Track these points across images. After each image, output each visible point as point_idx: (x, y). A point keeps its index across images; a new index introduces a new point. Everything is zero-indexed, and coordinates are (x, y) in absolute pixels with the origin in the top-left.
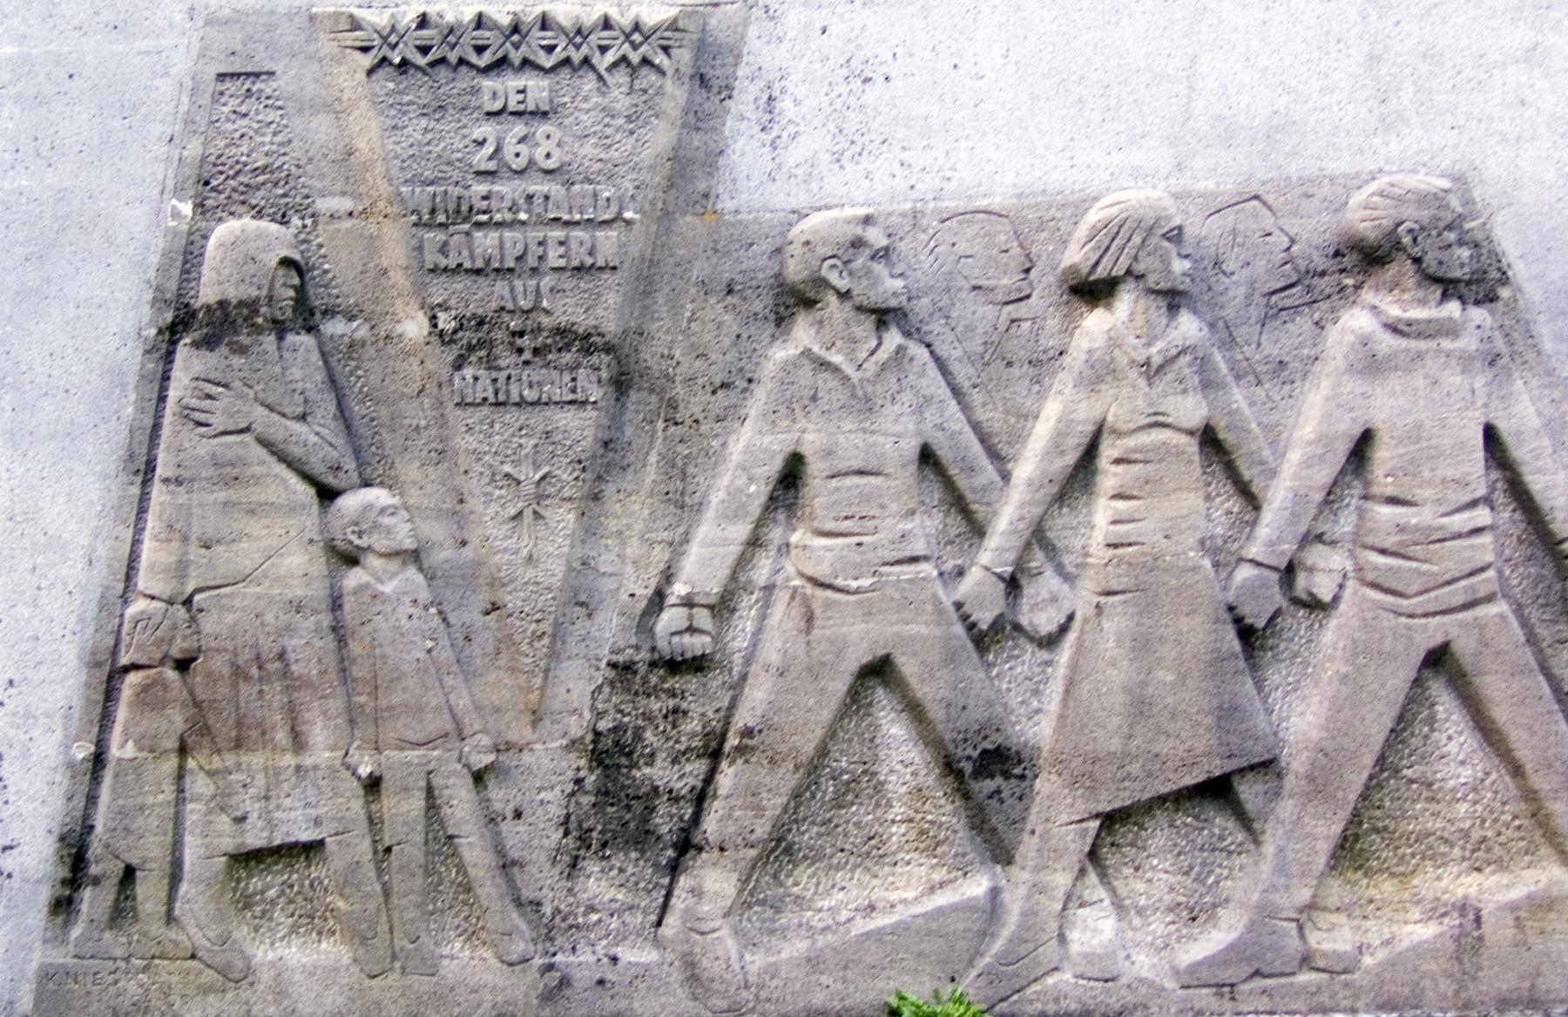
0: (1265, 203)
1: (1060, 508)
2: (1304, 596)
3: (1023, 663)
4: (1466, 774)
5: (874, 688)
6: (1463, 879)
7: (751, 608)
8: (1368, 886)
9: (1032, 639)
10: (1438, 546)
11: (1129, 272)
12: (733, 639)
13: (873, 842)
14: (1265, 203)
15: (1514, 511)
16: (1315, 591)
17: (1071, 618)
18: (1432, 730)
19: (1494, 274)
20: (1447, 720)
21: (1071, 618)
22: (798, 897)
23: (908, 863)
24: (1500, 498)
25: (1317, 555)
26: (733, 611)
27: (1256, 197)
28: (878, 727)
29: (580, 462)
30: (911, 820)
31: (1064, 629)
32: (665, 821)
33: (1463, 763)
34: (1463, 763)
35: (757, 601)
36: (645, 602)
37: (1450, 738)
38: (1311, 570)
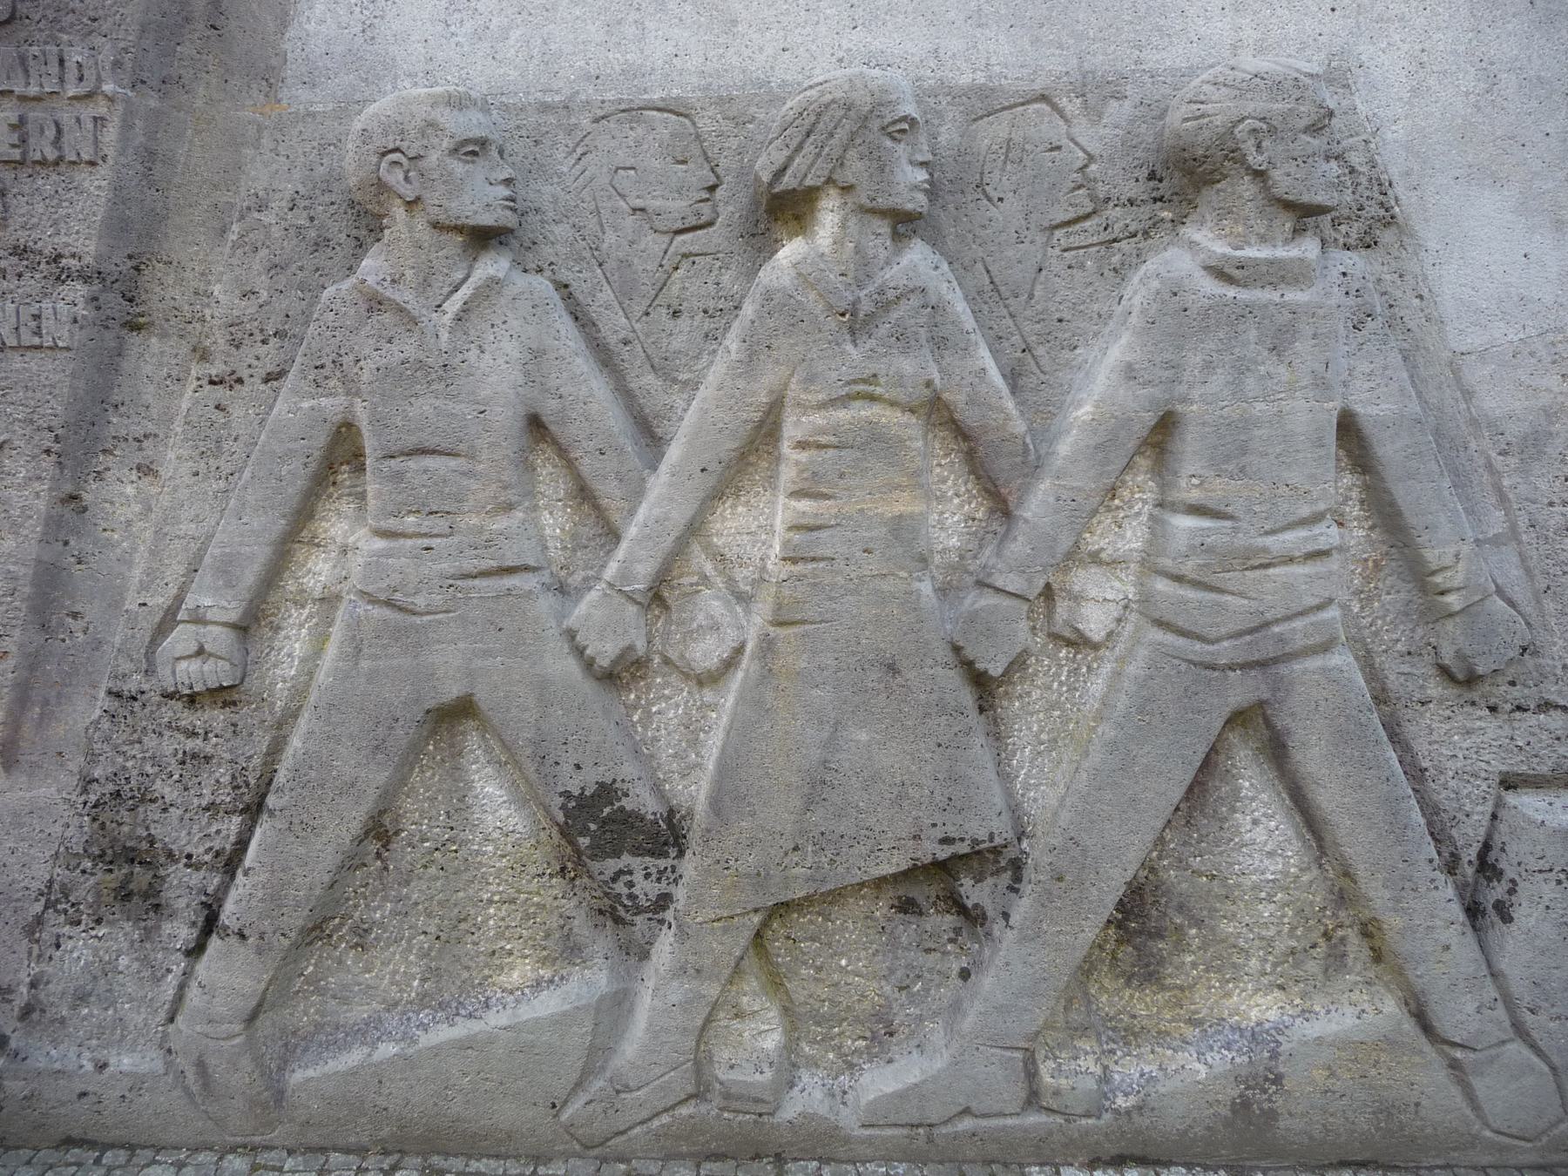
0: (1055, 107)
1: (734, 507)
2: (1067, 633)
3: (678, 706)
4: (1274, 867)
5: (463, 733)
6: (1258, 999)
7: (301, 626)
8: (1132, 997)
9: (687, 676)
10: (1258, 573)
11: (830, 181)
12: (275, 666)
13: (463, 926)
14: (1055, 107)
15: (1372, 528)
16: (1080, 626)
17: (739, 650)
18: (1233, 810)
19: (1373, 210)
20: (1253, 799)
21: (739, 650)
22: (369, 987)
23: (510, 953)
24: (1354, 510)
25: (1085, 580)
26: (278, 628)
27: (1043, 98)
28: (469, 785)
29: (50, 429)
30: (513, 901)
31: (730, 664)
32: (183, 887)
33: (1271, 854)
34: (1271, 854)
35: (310, 616)
36: (162, 613)
37: (1255, 822)
38: (1077, 598)
